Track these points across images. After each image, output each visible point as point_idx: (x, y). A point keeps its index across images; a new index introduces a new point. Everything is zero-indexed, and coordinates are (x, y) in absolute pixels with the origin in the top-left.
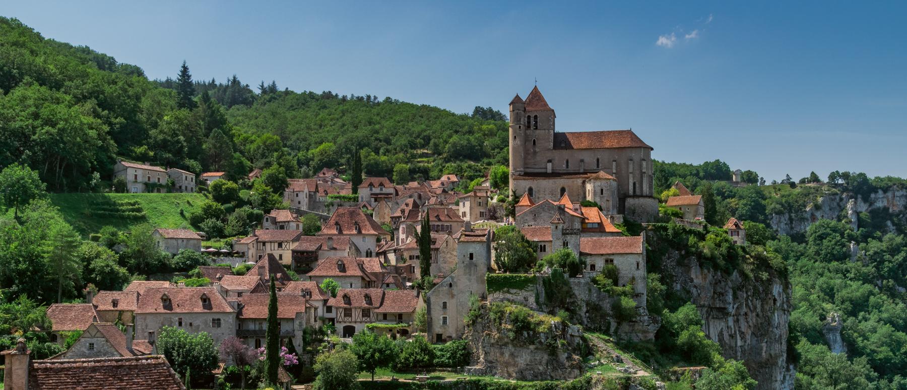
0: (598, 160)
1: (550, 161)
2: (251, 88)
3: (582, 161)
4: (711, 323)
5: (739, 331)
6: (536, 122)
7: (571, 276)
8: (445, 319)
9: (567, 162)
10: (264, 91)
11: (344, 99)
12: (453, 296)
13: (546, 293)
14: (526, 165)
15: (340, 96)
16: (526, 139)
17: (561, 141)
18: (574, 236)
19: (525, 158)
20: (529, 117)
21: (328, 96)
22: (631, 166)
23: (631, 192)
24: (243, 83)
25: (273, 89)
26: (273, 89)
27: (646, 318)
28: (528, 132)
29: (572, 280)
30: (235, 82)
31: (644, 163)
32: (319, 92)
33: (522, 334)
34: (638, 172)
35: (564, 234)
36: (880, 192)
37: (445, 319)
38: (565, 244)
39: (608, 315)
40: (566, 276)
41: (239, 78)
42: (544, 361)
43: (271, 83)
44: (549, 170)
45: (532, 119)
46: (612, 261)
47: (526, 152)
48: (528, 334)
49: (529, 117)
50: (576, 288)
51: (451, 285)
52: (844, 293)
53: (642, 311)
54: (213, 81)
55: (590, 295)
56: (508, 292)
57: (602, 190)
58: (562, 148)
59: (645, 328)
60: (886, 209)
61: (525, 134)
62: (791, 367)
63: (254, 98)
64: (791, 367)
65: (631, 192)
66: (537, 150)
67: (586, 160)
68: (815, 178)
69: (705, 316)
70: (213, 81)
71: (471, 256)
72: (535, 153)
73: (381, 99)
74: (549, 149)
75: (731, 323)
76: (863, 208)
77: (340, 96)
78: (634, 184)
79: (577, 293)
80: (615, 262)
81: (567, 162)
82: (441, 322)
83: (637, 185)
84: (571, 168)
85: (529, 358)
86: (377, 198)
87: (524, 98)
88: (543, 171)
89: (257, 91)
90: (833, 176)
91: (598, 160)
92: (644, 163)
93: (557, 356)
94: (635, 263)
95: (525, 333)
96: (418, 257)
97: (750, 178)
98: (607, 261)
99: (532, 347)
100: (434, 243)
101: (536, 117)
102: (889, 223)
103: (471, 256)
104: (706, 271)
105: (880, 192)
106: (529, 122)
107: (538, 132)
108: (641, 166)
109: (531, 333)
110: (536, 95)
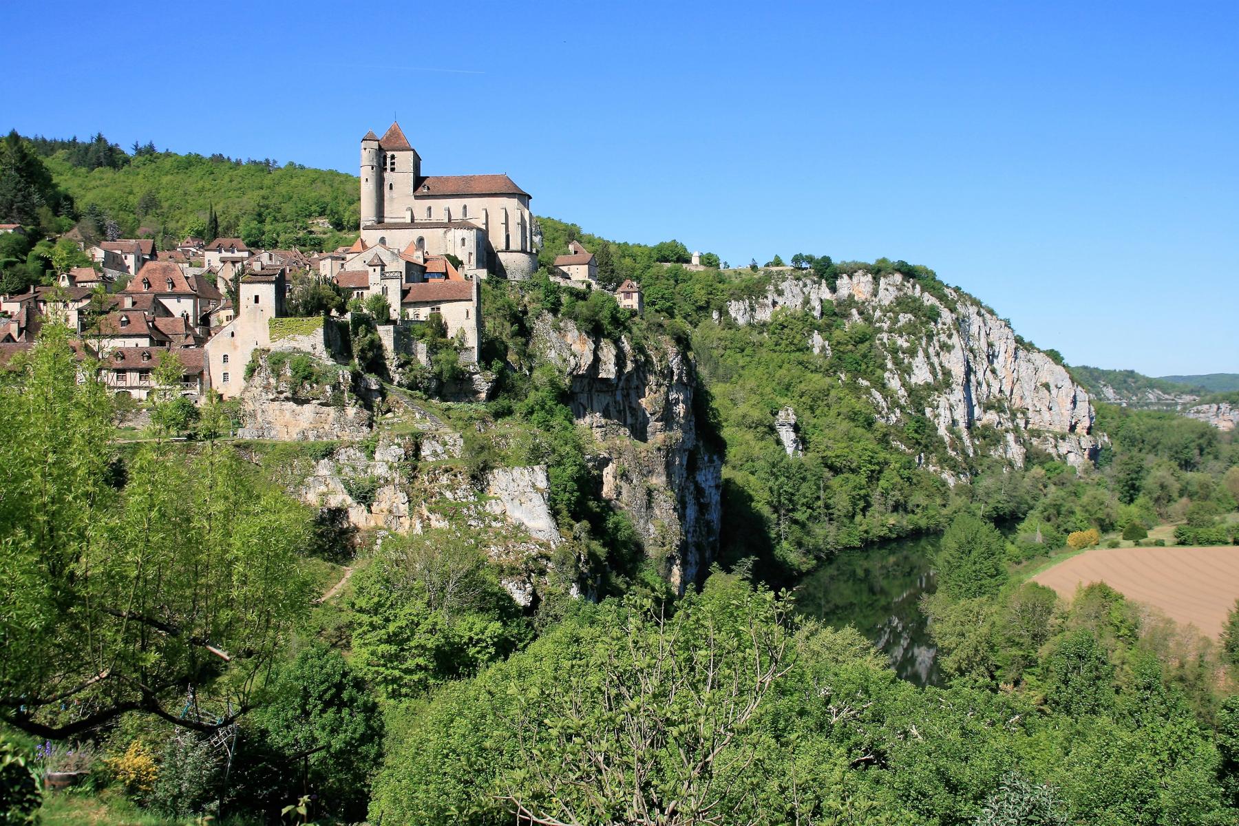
0: (465, 207)
2: (122, 148)
4: (595, 398)
5: (630, 407)
6: (393, 164)
10: (139, 152)
11: (238, 163)
12: (235, 348)
15: (233, 160)
21: (218, 159)
24: (111, 141)
25: (150, 150)
26: (150, 150)
30: (100, 139)
32: (207, 154)
36: (845, 276)
38: (385, 290)
41: (104, 136)
43: (147, 143)
51: (233, 335)
52: (803, 387)
54: (75, 139)
56: (293, 339)
57: (463, 240)
60: (851, 296)
62: (715, 457)
63: (127, 161)
64: (715, 457)
66: (395, 196)
68: (778, 263)
69: (586, 389)
70: (75, 139)
71: (257, 299)
73: (282, 164)
75: (619, 398)
76: (826, 294)
77: (233, 160)
80: (442, 311)
84: (434, 219)
86: (224, 261)
89: (130, 152)
90: (797, 259)
91: (465, 207)
97: (709, 261)
101: (393, 157)
102: (854, 311)
103: (257, 299)
105: (845, 276)
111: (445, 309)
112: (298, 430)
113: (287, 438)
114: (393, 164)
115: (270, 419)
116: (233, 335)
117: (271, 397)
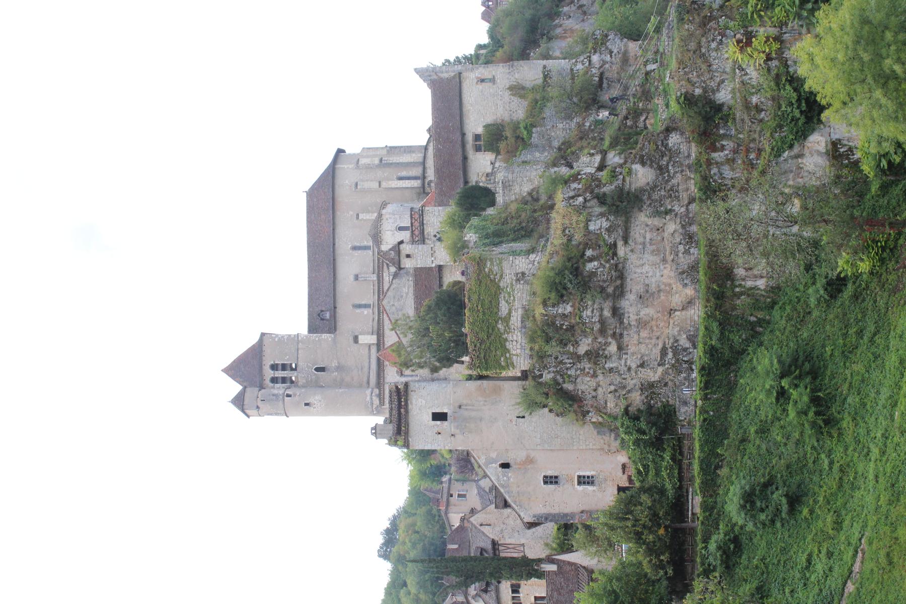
0: (355, 248)
1: (356, 339)
3: (356, 277)
6: (284, 367)
7: (493, 203)
8: (584, 481)
9: (360, 306)
12: (530, 461)
13: (514, 240)
14: (361, 386)
16: (317, 385)
17: (323, 317)
18: (426, 218)
19: (349, 386)
20: (274, 380)
22: (367, 185)
23: (417, 183)
27: (595, 58)
28: (301, 382)
29: (500, 199)
31: (363, 161)
33: (593, 274)
34: (380, 174)
35: (423, 241)
37: (584, 481)
39: (580, 126)
40: (490, 211)
42: (656, 222)
44: (373, 339)
45: (280, 374)
46: (477, 137)
47: (340, 384)
48: (591, 260)
49: (274, 380)
50: (517, 189)
51: (505, 466)
53: (580, 66)
55: (536, 162)
56: (507, 319)
58: (334, 316)
59: (617, 59)
61: (303, 387)
65: (417, 183)
66: (334, 364)
67: (356, 271)
71: (439, 417)
72: (339, 368)
74: (334, 340)
78: (401, 178)
79: (527, 188)
80: (480, 130)
81: (360, 306)
82: (590, 488)
83: (404, 174)
84: (370, 298)
85: (648, 257)
87: (236, 388)
88: (374, 350)
91: (355, 248)
92: (363, 161)
93: (642, 190)
94: (481, 86)
95: (590, 266)
96: (515, 589)
98: (478, 149)
99: (621, 251)
100: (483, 550)
101: (274, 367)
103: (439, 417)
104: (558, 31)
106: (284, 380)
107: (300, 364)
108: (368, 167)
109: (589, 253)
110: (235, 370)
111: (475, 125)
112: (677, 286)
113: (697, 313)
114: (284, 367)
115: (657, 352)
116: (505, 466)
117: (613, 348)
